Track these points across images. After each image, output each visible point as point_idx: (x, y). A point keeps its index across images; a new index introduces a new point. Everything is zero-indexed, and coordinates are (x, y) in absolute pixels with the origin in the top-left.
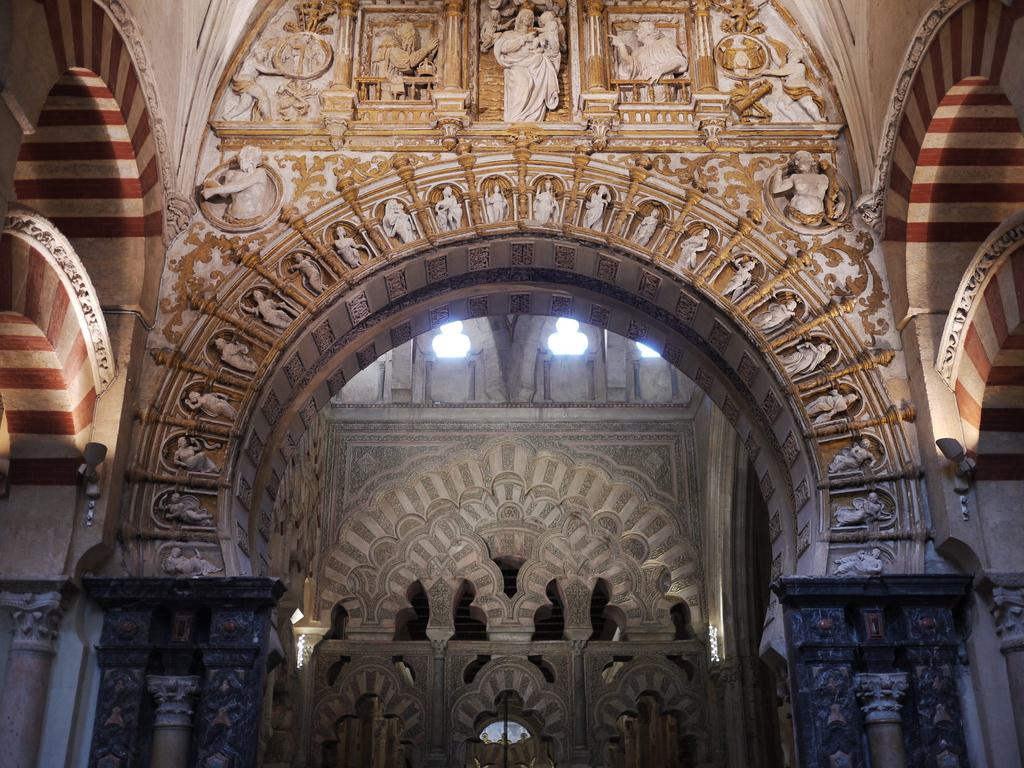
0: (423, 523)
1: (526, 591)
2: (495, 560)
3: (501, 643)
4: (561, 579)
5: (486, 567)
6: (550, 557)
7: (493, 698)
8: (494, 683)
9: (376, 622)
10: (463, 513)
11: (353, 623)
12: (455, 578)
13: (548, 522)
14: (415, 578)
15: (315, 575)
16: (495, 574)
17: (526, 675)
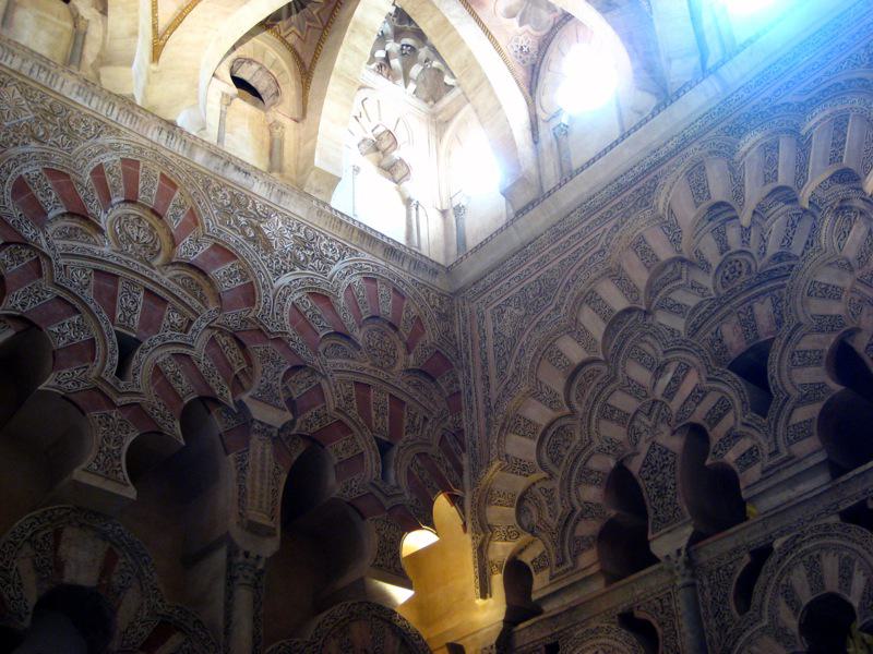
0: (604, 369)
1: (789, 389)
2: (729, 368)
3: (780, 512)
4: (852, 332)
5: (717, 385)
6: (818, 307)
7: (792, 624)
8: (789, 593)
9: (570, 564)
10: (663, 318)
11: (540, 583)
12: (674, 433)
13: (797, 248)
14: (612, 463)
15: (469, 526)
16: (733, 389)
17: (846, 553)
